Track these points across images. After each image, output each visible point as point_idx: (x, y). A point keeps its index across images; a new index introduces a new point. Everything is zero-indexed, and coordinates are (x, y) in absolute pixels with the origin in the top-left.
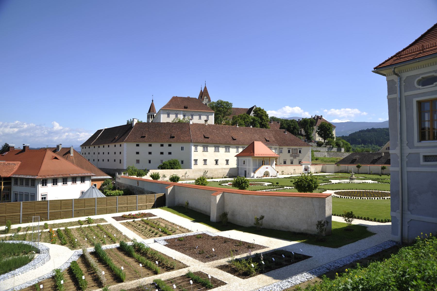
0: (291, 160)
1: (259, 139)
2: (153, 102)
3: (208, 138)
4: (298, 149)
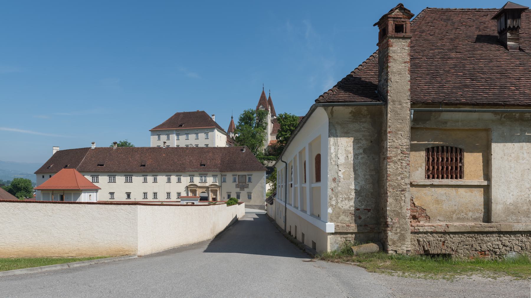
0: (237, 193)
1: (190, 162)
2: (233, 119)
3: (103, 165)
4: (247, 176)
